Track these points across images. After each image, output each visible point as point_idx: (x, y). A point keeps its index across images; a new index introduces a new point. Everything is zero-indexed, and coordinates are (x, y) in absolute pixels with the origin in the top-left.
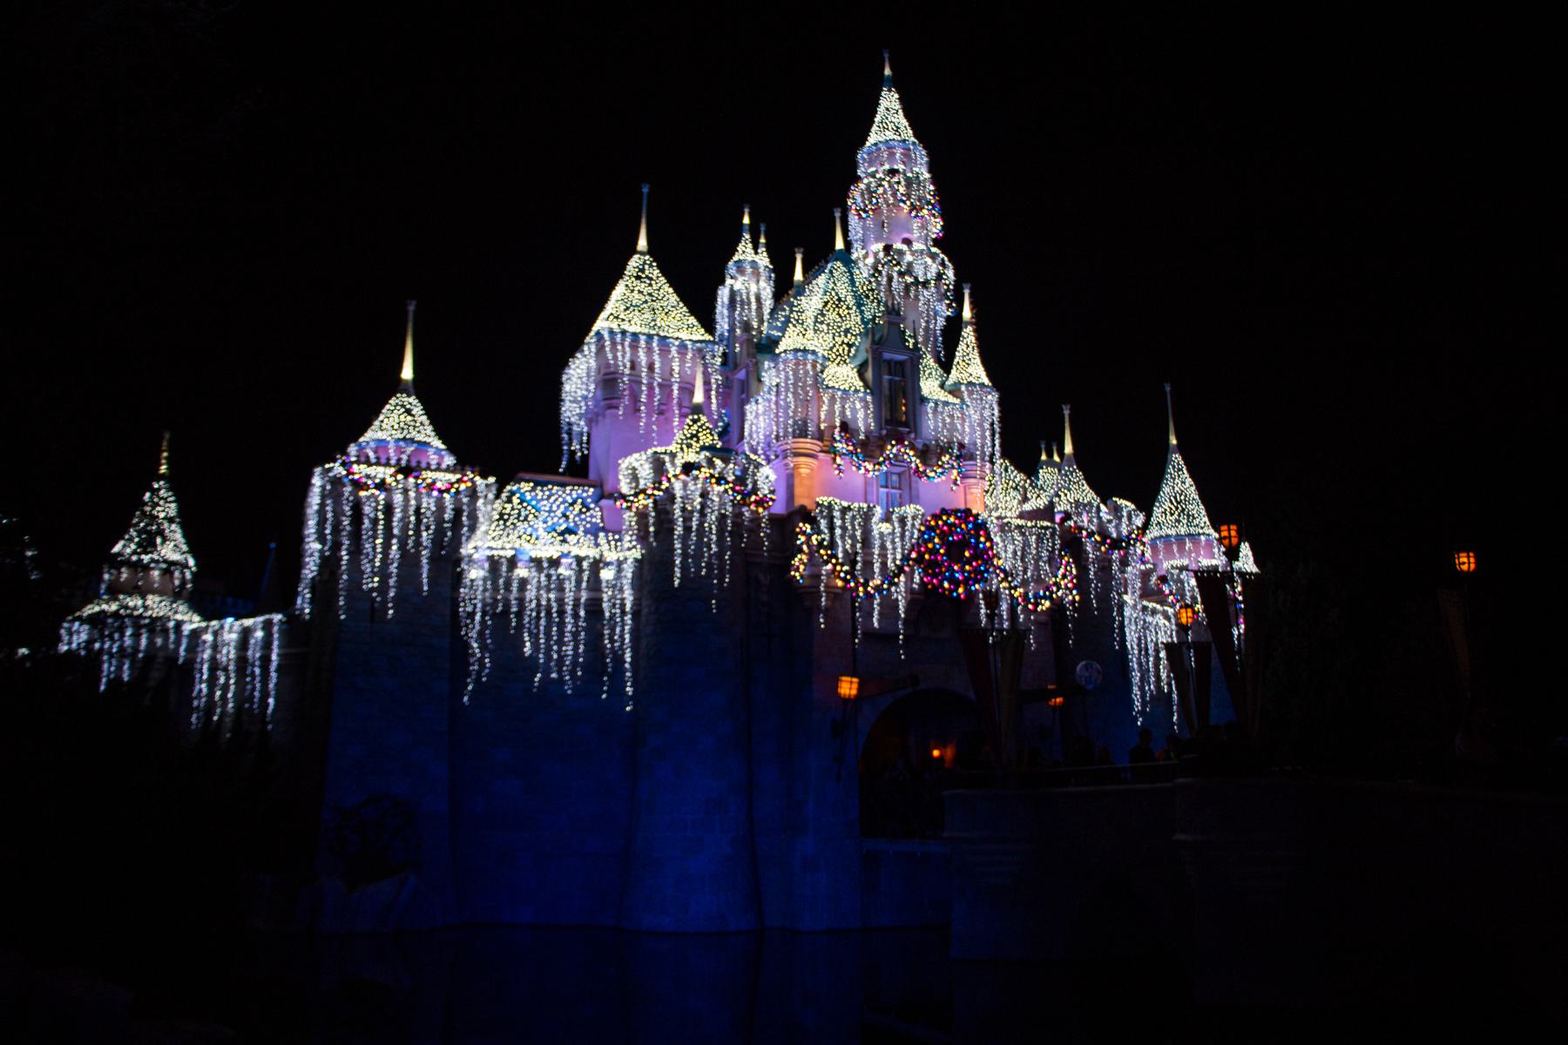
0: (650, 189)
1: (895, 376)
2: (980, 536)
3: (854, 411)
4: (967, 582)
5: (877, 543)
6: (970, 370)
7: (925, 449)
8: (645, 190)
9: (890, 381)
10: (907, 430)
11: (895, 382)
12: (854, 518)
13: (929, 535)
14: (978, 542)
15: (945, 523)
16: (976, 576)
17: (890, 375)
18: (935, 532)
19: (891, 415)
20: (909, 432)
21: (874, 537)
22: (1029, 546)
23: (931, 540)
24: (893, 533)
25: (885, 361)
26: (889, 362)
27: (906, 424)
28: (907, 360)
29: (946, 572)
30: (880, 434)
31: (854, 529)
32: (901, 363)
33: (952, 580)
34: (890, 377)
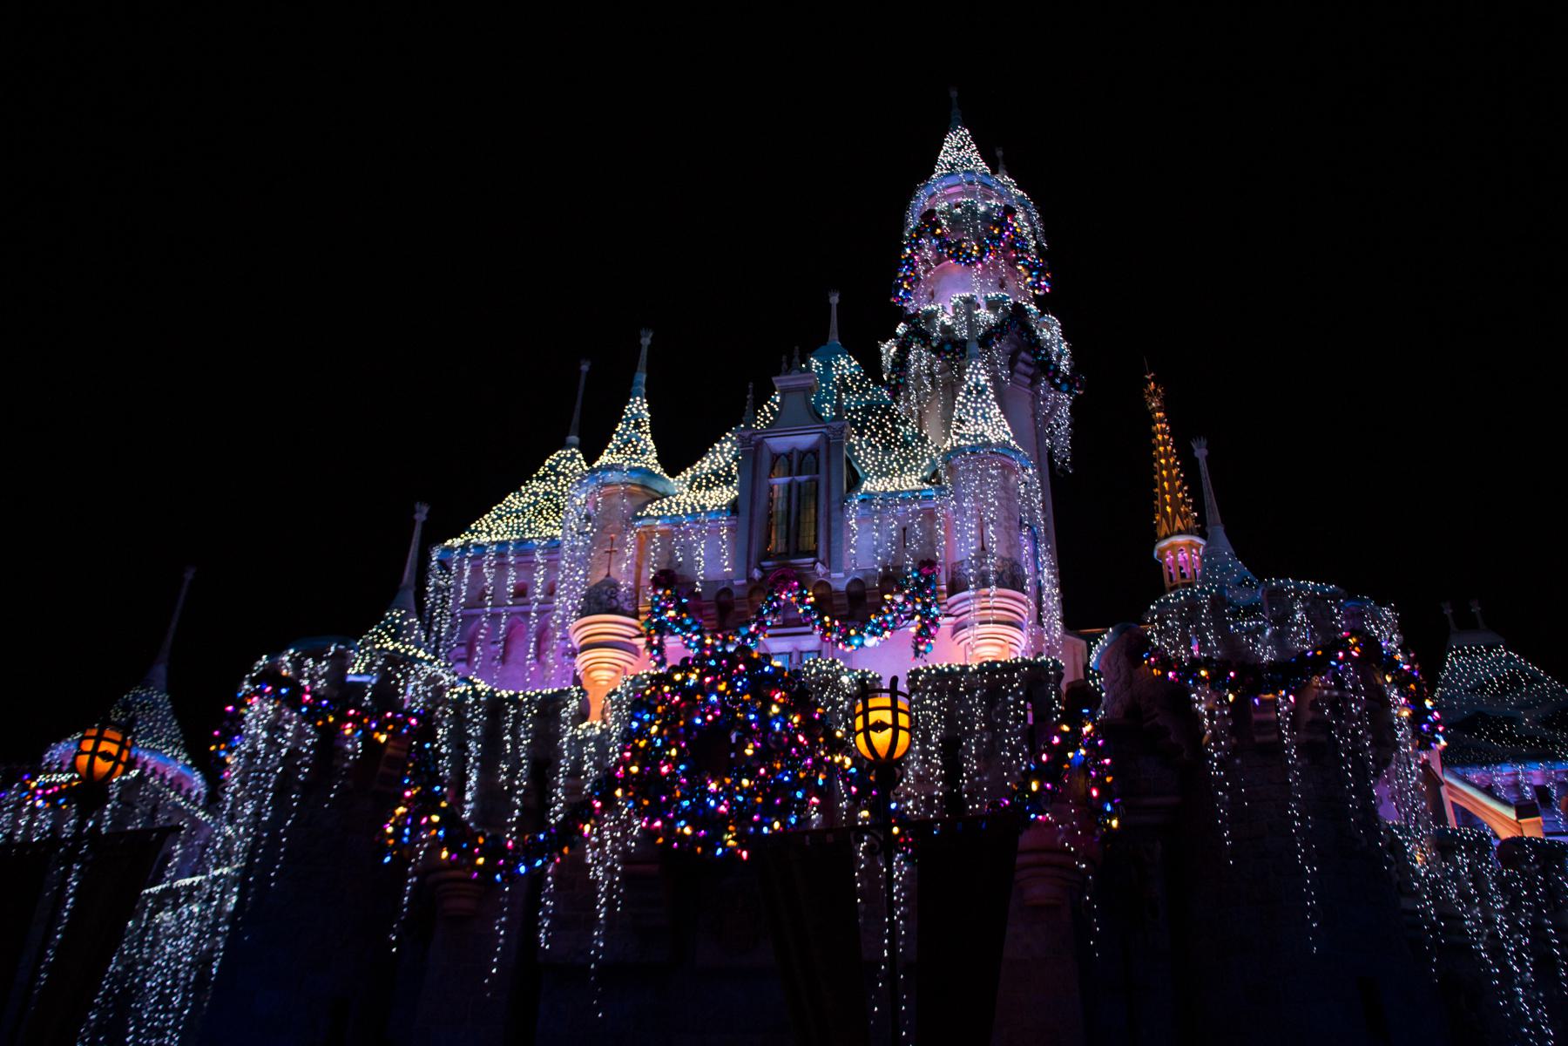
0: (590, 367)
1: (800, 473)
2: (769, 701)
3: (688, 549)
4: (740, 816)
5: (565, 766)
6: (964, 430)
7: (854, 589)
8: (585, 367)
9: (790, 485)
10: (812, 560)
11: (799, 485)
12: (518, 718)
13: (640, 720)
14: (765, 720)
15: (680, 688)
16: (768, 799)
17: (789, 475)
18: (652, 710)
19: (787, 543)
20: (815, 563)
21: (560, 751)
22: (969, 719)
23: (642, 732)
24: (606, 732)
25: (776, 457)
26: (788, 456)
27: (814, 554)
28: (817, 443)
29: (683, 798)
30: (750, 579)
31: (516, 742)
32: (813, 451)
33: (699, 816)
34: (787, 479)
